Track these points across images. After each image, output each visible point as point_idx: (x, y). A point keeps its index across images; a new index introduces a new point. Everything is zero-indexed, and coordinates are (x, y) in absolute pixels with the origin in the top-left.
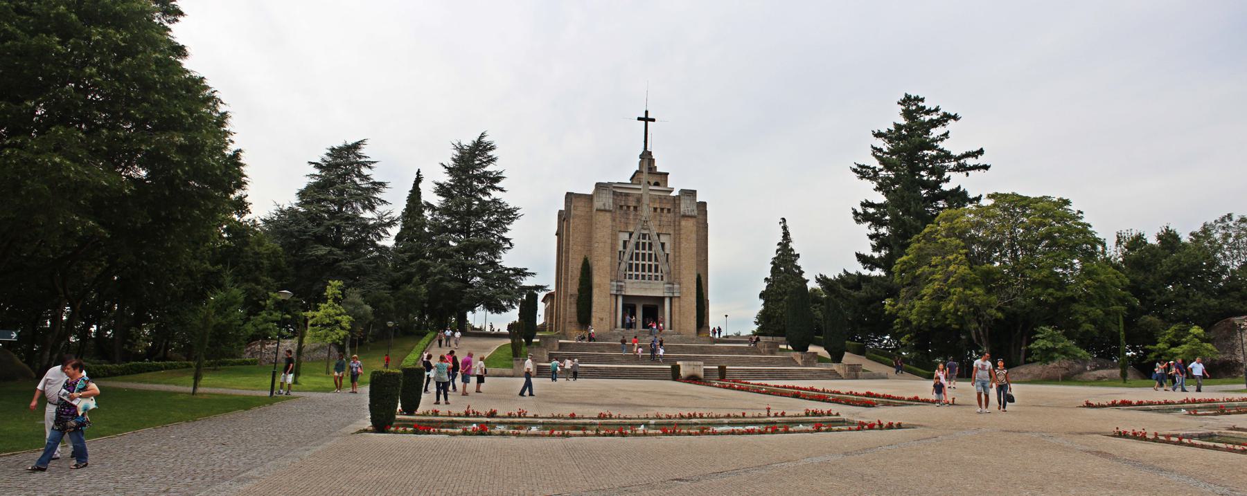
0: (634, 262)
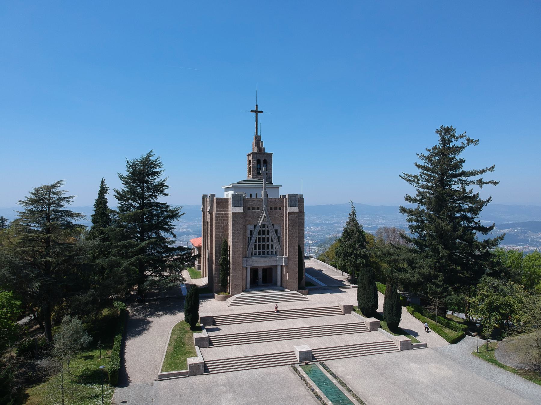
0: (258, 243)
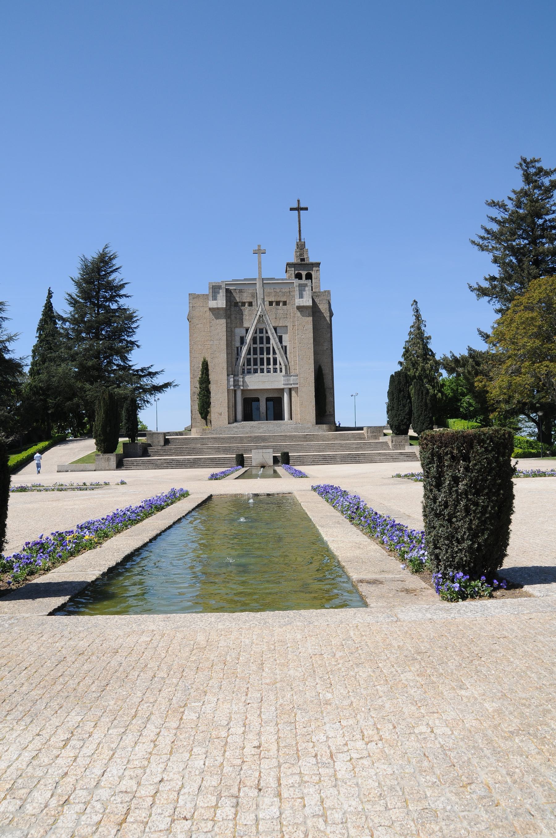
0: (252, 356)
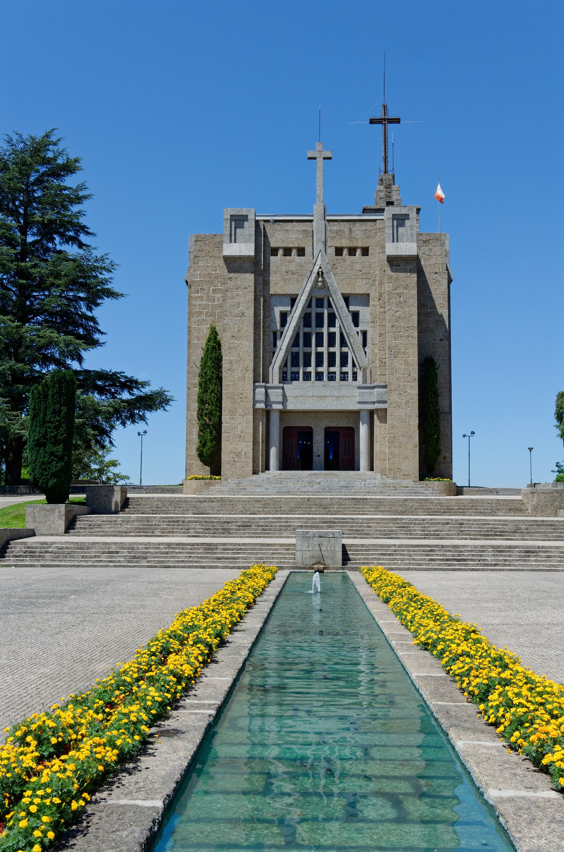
0: (301, 349)
